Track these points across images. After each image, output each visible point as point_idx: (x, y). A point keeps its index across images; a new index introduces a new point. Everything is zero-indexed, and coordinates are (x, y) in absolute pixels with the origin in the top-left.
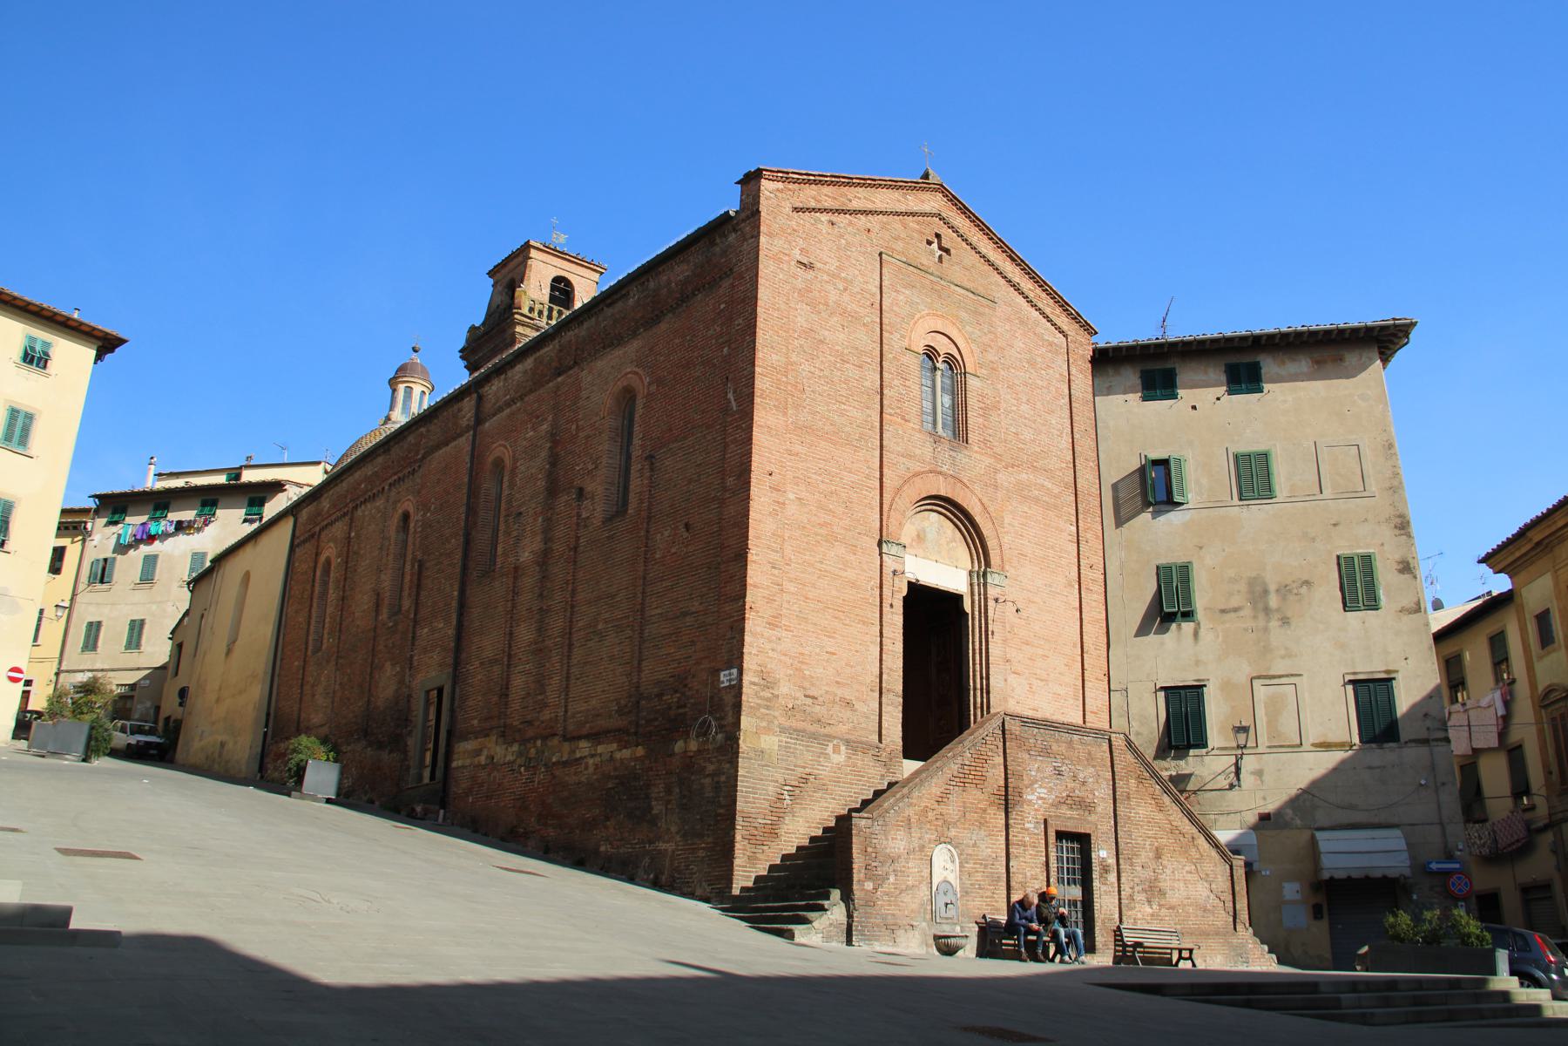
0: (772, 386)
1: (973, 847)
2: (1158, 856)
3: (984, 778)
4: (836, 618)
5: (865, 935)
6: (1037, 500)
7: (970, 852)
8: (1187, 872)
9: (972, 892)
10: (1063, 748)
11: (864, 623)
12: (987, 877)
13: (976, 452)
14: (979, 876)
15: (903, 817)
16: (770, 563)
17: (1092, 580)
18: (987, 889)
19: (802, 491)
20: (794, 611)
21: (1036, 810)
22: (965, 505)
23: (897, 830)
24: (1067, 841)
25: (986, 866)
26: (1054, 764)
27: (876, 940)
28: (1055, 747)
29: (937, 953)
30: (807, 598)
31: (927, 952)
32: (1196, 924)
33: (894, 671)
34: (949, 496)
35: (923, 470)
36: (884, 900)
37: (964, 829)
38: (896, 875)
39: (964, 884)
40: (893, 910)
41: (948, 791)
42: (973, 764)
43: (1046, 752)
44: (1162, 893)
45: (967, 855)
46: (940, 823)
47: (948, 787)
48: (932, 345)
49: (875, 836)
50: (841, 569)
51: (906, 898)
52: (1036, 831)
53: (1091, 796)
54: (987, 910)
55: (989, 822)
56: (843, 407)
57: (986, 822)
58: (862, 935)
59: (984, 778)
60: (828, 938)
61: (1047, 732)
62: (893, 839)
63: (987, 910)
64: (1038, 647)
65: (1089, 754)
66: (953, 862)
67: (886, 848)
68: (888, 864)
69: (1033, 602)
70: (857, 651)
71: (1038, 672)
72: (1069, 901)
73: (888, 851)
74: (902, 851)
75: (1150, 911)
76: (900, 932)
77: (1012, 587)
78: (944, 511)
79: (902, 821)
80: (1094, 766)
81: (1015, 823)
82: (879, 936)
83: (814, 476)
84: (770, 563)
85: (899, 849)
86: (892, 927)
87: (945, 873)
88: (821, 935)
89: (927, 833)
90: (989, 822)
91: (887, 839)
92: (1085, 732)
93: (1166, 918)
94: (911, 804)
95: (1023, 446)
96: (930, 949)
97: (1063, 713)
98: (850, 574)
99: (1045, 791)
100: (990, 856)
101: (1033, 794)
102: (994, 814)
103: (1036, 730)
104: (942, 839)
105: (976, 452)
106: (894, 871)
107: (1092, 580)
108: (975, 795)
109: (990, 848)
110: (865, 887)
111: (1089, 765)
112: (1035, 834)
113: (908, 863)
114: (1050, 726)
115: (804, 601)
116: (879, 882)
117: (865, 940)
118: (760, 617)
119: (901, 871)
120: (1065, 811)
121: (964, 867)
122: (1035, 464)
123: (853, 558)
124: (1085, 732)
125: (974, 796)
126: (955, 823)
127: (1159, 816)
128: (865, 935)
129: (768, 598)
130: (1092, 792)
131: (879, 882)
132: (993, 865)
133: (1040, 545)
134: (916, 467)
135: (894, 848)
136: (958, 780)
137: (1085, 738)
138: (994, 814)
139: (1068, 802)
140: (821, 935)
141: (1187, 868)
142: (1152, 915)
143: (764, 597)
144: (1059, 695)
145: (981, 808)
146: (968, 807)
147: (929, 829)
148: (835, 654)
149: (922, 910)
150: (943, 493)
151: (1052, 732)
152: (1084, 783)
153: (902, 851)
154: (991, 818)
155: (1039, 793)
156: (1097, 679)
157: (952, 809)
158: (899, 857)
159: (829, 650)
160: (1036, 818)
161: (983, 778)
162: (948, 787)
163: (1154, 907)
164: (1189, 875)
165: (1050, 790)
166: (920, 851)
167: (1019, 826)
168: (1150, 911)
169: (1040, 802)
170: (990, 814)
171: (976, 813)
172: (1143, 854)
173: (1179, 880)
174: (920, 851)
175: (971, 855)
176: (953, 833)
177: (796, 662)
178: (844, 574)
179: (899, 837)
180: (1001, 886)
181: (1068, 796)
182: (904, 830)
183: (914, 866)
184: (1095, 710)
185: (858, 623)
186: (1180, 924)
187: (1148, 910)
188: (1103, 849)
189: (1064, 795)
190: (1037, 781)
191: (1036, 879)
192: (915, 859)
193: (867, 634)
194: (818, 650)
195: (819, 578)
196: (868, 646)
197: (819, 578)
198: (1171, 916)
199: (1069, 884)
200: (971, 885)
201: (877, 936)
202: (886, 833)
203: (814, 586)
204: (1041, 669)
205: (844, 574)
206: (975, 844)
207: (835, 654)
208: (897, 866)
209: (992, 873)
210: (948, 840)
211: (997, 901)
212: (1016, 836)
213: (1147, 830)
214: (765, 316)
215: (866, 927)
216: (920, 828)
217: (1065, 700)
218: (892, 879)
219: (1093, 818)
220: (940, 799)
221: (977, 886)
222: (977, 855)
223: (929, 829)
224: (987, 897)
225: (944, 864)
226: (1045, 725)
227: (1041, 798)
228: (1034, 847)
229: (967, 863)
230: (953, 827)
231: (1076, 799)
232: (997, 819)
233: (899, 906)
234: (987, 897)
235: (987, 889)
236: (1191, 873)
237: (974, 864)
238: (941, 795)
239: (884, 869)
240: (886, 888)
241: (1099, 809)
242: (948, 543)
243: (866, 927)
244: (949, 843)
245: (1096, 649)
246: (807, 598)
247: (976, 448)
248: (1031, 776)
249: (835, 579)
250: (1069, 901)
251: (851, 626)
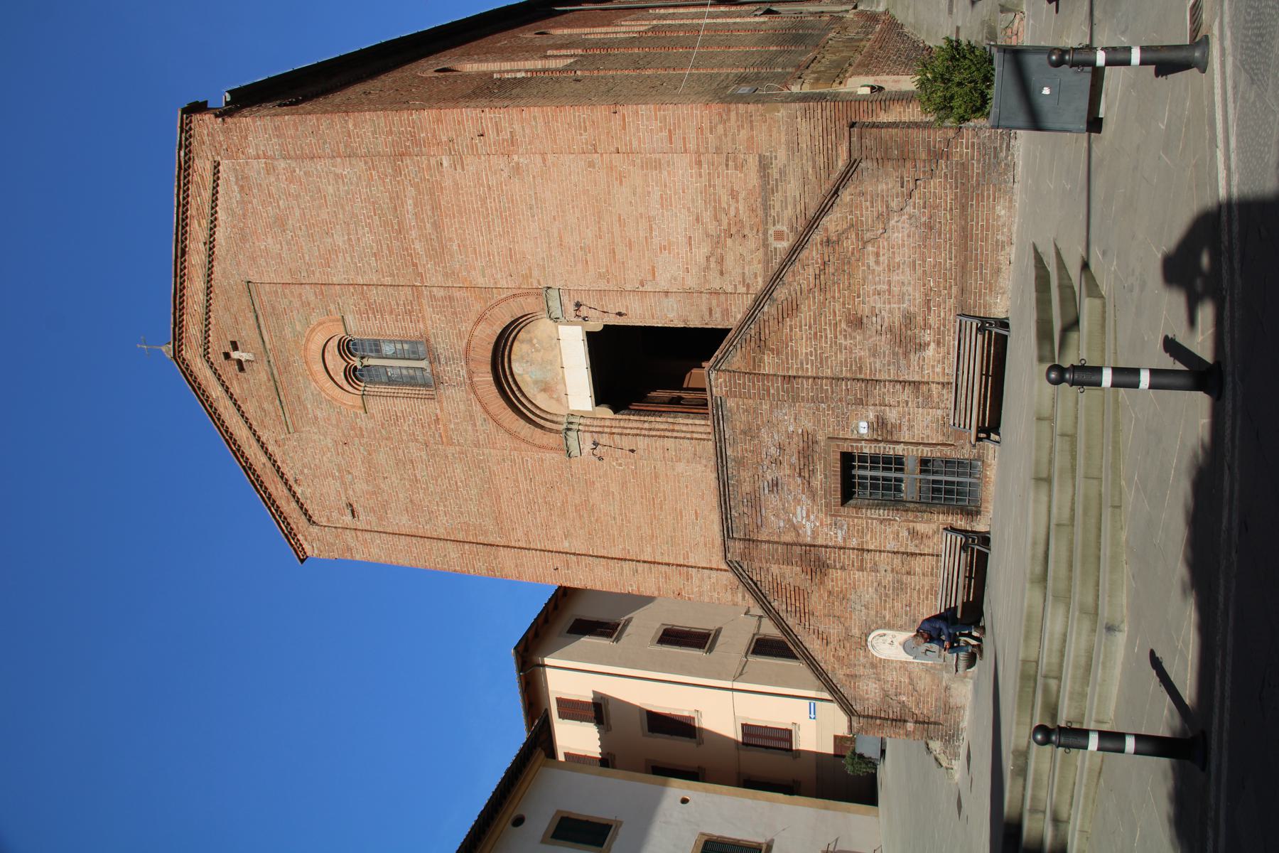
0: (479, 559)
1: (868, 609)
2: (857, 323)
3: (797, 589)
4: (661, 508)
5: (954, 734)
6: (436, 225)
7: (873, 613)
8: (877, 263)
9: (914, 615)
10: (745, 474)
11: (656, 477)
12: (898, 595)
13: (425, 324)
14: (898, 605)
15: (846, 681)
16: (634, 575)
17: (498, 135)
18: (911, 596)
19: (557, 532)
20: (668, 548)
21: (821, 524)
22: (491, 347)
23: (859, 688)
24: (854, 467)
25: (886, 595)
26: (766, 491)
27: (958, 725)
28: (747, 488)
29: (973, 669)
30: (653, 536)
31: (971, 679)
32: (950, 252)
33: (695, 451)
34: (489, 368)
35: (478, 403)
36: (924, 707)
37: (851, 618)
38: (900, 694)
39: (905, 624)
40: (932, 700)
41: (816, 631)
42: (784, 600)
43: (755, 502)
44: (909, 319)
45: (876, 616)
46: (848, 645)
47: (811, 631)
48: (342, 374)
49: (866, 709)
50: (613, 498)
51: (921, 686)
52: (845, 527)
53: (795, 439)
54: (931, 599)
55: (842, 588)
56: (459, 484)
57: (842, 591)
58: (953, 736)
59: (797, 589)
60: (956, 756)
61: (732, 496)
62: (867, 693)
63: (931, 599)
64: (612, 233)
65: (744, 433)
66: (885, 635)
67: (876, 701)
68: (891, 701)
69: (561, 238)
70: (687, 487)
71: (642, 234)
72: (922, 471)
73: (879, 700)
74: (877, 686)
75: (933, 345)
76: (952, 701)
77: (554, 275)
78: (509, 377)
79: (850, 682)
80: (759, 429)
81: (839, 563)
82: (955, 721)
83: (538, 519)
84: (634, 575)
85: (876, 688)
86: (947, 708)
87: (896, 643)
88: (953, 761)
89: (859, 660)
90: (842, 588)
91: (868, 699)
92: (720, 441)
93: (942, 314)
94: (833, 671)
95: (385, 247)
96: (969, 675)
97: (684, 192)
98: (614, 488)
99: (799, 508)
100: (876, 590)
101: (804, 526)
102: (832, 581)
103: (733, 512)
104: (863, 643)
105: (425, 324)
106: (896, 695)
107: (498, 135)
108: (815, 602)
109: (867, 590)
110: (912, 730)
111: (758, 437)
112: (849, 529)
113: (888, 681)
114: (725, 495)
115: (657, 539)
116: (907, 710)
117: (958, 734)
118: (684, 588)
119: (896, 689)
120: (819, 478)
121: (889, 621)
122: (396, 227)
123: (598, 485)
124: (720, 441)
125: (817, 601)
126: (847, 629)
127: (806, 313)
128: (954, 734)
129: (666, 578)
130: (789, 436)
131: (907, 710)
132: (885, 587)
133: (489, 227)
134: (477, 408)
135: (875, 693)
136: (803, 619)
137: (727, 437)
138: (832, 581)
139: (807, 475)
140: (953, 761)
141: (871, 260)
142: (938, 343)
143: (666, 582)
144: (662, 198)
145: (828, 597)
146: (829, 610)
147: (855, 656)
148: (696, 512)
149: (932, 671)
150: (490, 378)
151: (731, 488)
152: (780, 447)
153: (877, 686)
154: (837, 586)
155: (802, 518)
156: (624, 128)
157: (834, 630)
158: (883, 689)
159: (694, 517)
160: (831, 524)
161: (797, 590)
162: (811, 631)
163: (927, 339)
164: (881, 259)
165: (798, 501)
166: (876, 667)
167: (842, 556)
168: (933, 345)
169: (812, 517)
170: (833, 586)
171: (833, 604)
172: (858, 352)
173: (889, 283)
174: (876, 667)
175: (877, 612)
176: (856, 632)
177: (714, 550)
178: (617, 497)
179: (865, 687)
180: (907, 580)
181: (800, 475)
182: (859, 682)
183: (891, 676)
184: (665, 134)
185: (659, 483)
186: (951, 287)
187: (931, 351)
188: (857, 427)
189: (799, 480)
190: (789, 520)
191: (898, 536)
192: (884, 673)
193: (667, 475)
194: (697, 528)
195: (630, 522)
196: (678, 474)
197: (630, 522)
198: (939, 306)
199: (902, 470)
200: (906, 615)
201: (954, 724)
202: (863, 699)
203: (639, 528)
204: (638, 230)
205: (617, 497)
206: (865, 606)
207: (696, 512)
208: (892, 692)
209: (893, 590)
210: (864, 637)
211: (923, 587)
212: (853, 562)
213: (826, 343)
214: (422, 561)
215: (946, 733)
216: (855, 665)
217: (665, 186)
218: (904, 698)
219: (821, 437)
220: (825, 641)
221: (908, 609)
222: (877, 608)
223: (855, 656)
224: (919, 598)
225: (887, 646)
226: (725, 503)
227: (808, 516)
228: (862, 532)
229: (884, 618)
230: (851, 630)
231: (802, 463)
232: (837, 579)
233: (928, 694)
234: (919, 598)
235: (911, 596)
236: (877, 255)
237: (885, 609)
238: (820, 639)
239: (894, 705)
240: (911, 704)
241: (809, 426)
242: (537, 351)
243: (946, 733)
244: (867, 635)
245: (585, 131)
246: (653, 536)
247: (422, 326)
248: (785, 527)
249: (625, 506)
250: (922, 471)
251: (664, 491)
